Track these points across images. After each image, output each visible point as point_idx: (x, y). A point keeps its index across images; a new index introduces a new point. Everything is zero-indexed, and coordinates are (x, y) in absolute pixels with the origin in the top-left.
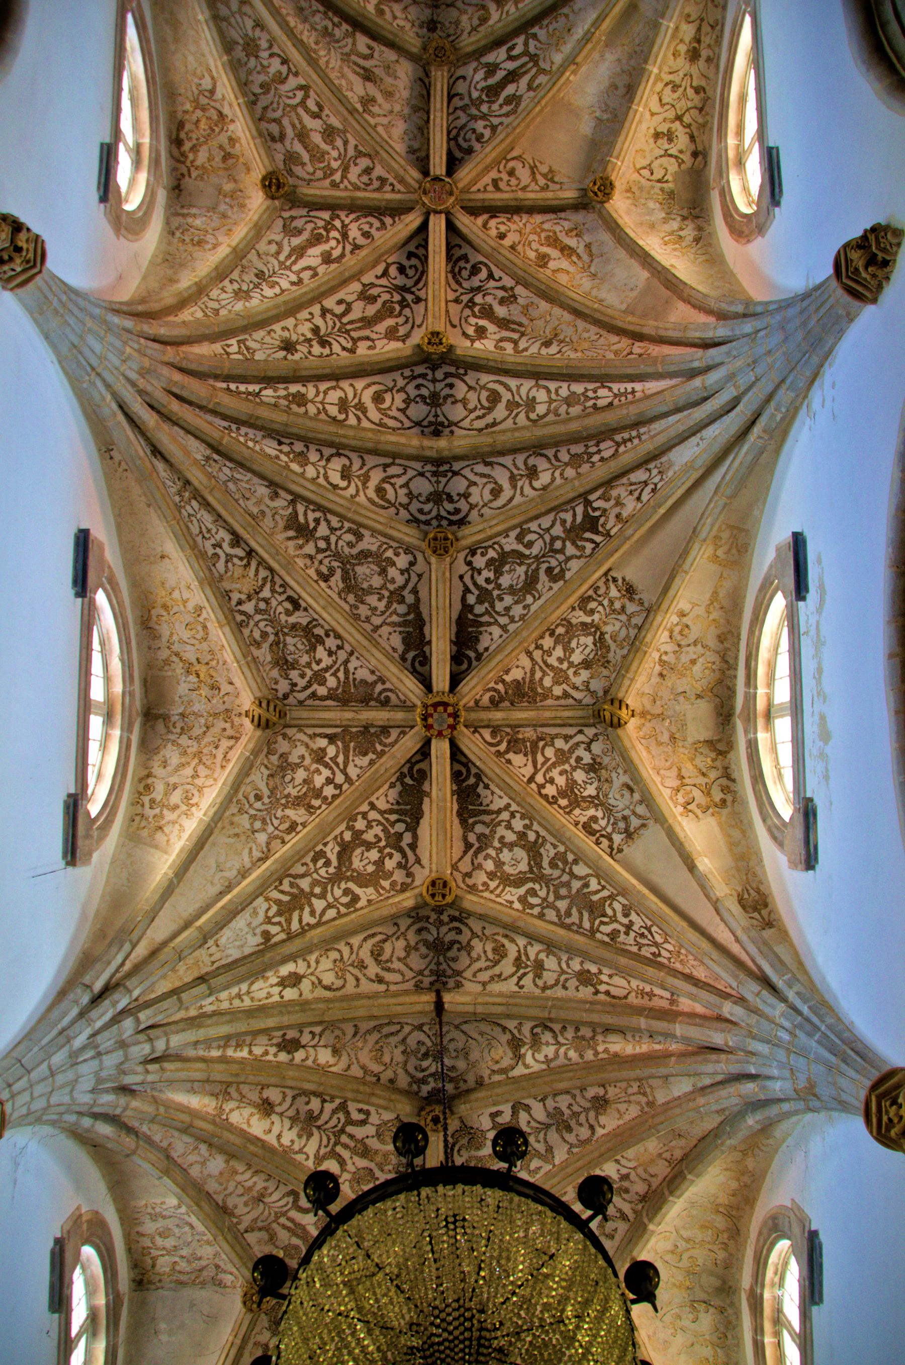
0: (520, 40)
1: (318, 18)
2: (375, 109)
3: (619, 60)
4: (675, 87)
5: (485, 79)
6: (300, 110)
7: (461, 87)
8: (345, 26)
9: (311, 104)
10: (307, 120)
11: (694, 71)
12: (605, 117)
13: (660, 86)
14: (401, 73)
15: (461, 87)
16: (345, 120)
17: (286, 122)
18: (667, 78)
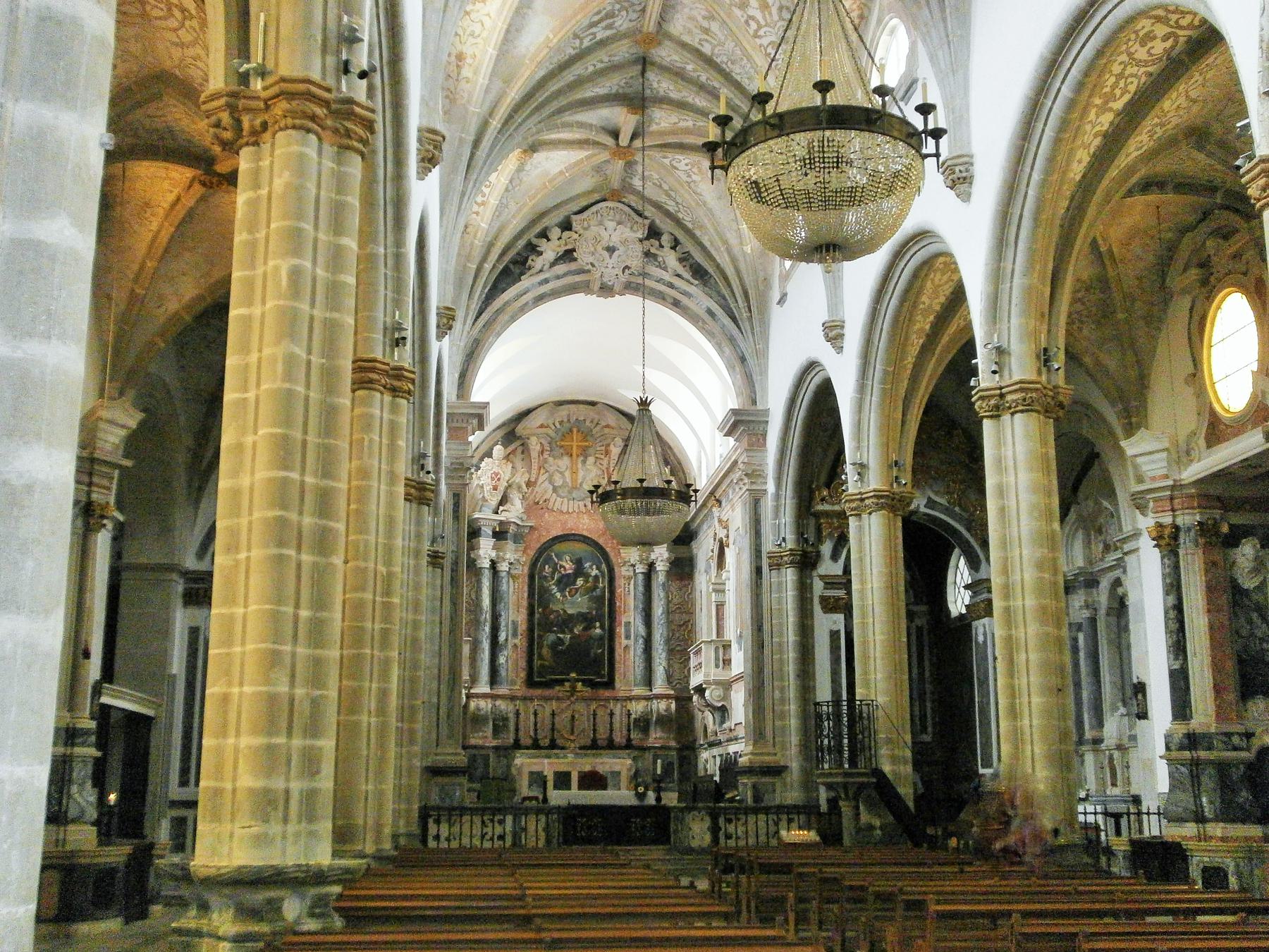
0: (586, 43)
1: (738, 71)
2: (704, 13)
3: (515, 48)
4: (472, 35)
5: (614, 22)
6: (763, 23)
7: (635, 16)
8: (718, 60)
9: (754, 25)
10: (759, 16)
11: (459, 47)
12: (525, 11)
13: (485, 34)
14: (681, 29)
15: (635, 16)
16: (729, 15)
17: (776, 18)
18: (479, 40)
